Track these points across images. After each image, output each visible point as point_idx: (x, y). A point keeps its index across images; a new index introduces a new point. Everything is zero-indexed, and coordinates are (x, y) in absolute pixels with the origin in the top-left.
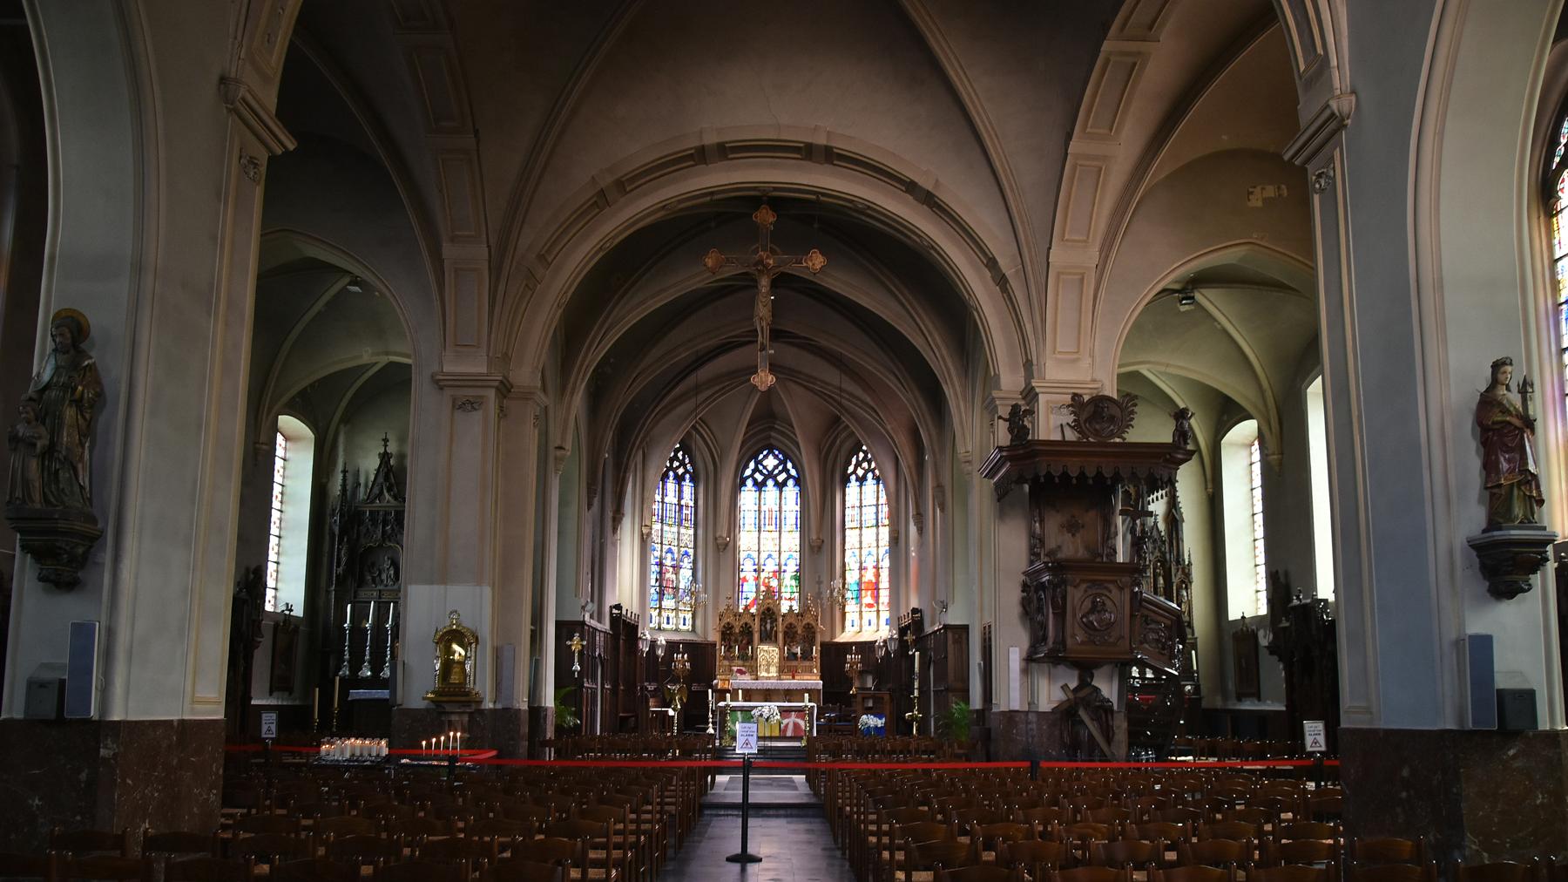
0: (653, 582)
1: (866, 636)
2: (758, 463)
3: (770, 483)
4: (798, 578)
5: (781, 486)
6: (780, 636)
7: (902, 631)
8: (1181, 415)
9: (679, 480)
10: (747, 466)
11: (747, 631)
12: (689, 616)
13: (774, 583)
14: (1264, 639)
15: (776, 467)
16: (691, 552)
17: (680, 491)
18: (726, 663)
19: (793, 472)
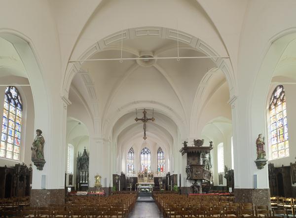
4: (150, 167)
5: (147, 154)
7: (167, 175)
8: (211, 142)
11: (142, 176)
14: (224, 175)
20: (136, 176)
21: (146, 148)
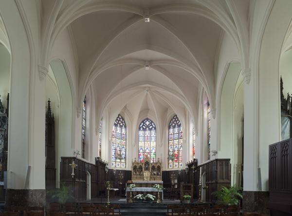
0: (113, 154)
1: (176, 168)
2: (144, 123)
3: (147, 128)
5: (150, 130)
6: (150, 169)
9: (121, 127)
10: (141, 124)
11: (141, 168)
12: (124, 164)
13: (149, 156)
15: (149, 124)
16: (125, 147)
17: (122, 130)
19: (154, 126)
20: (129, 168)
21: (147, 119)
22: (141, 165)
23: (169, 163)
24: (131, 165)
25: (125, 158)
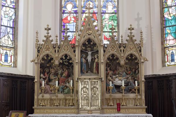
6: (102, 68)
11: (67, 64)
12: (11, 53)
18: (47, 96)
20: (25, 66)
22: (70, 53)
23: (164, 49)
24: (32, 54)
25: (15, 28)
